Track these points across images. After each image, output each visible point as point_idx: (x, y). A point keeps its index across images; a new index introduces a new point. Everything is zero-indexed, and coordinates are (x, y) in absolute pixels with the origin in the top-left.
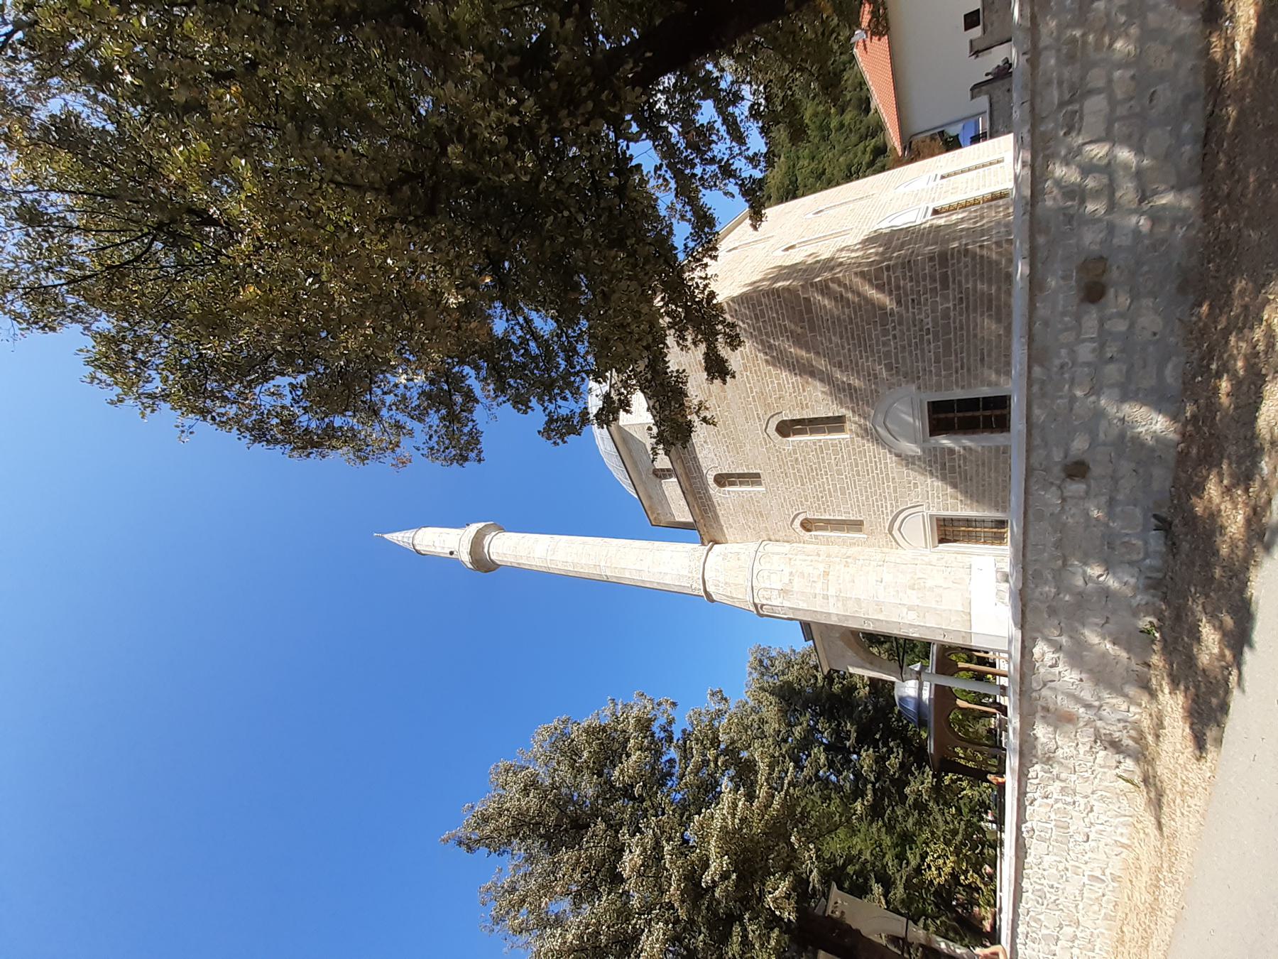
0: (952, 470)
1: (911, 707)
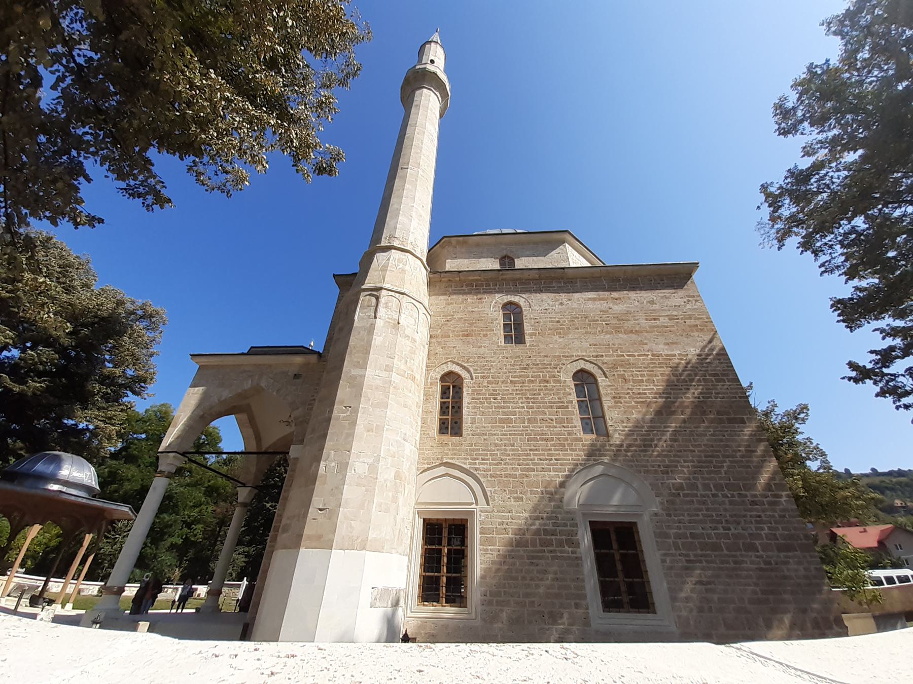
0: (544, 543)
1: (40, 467)
